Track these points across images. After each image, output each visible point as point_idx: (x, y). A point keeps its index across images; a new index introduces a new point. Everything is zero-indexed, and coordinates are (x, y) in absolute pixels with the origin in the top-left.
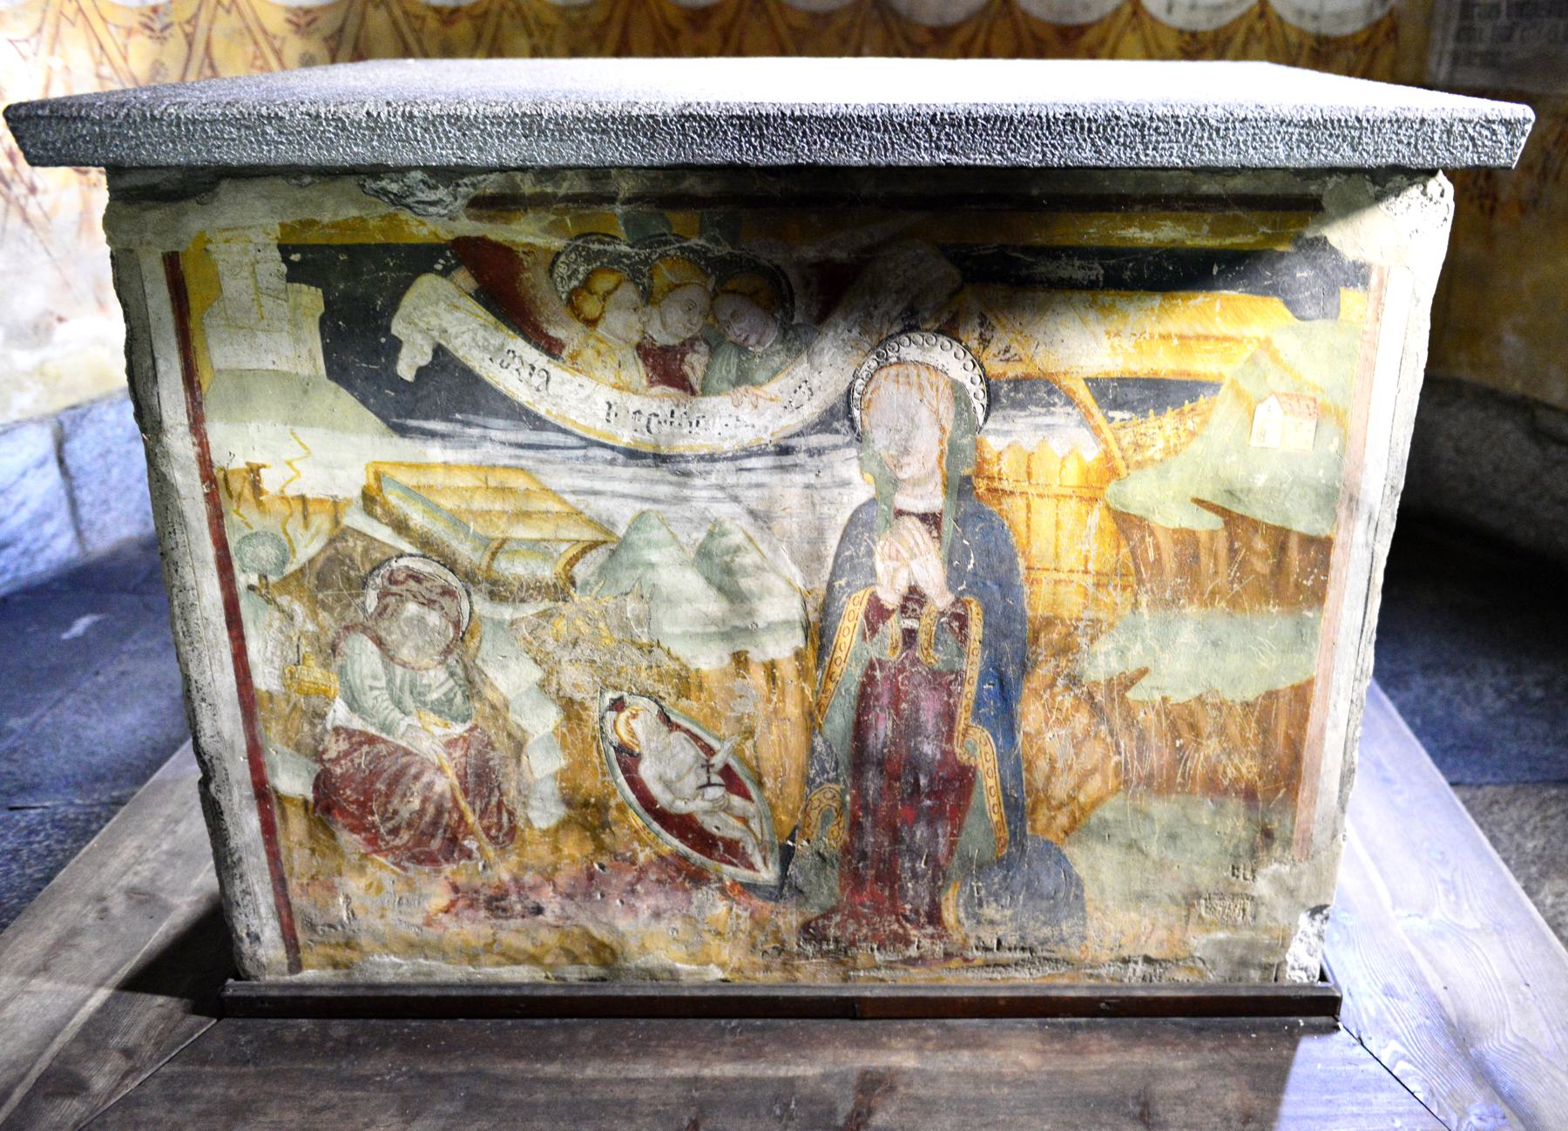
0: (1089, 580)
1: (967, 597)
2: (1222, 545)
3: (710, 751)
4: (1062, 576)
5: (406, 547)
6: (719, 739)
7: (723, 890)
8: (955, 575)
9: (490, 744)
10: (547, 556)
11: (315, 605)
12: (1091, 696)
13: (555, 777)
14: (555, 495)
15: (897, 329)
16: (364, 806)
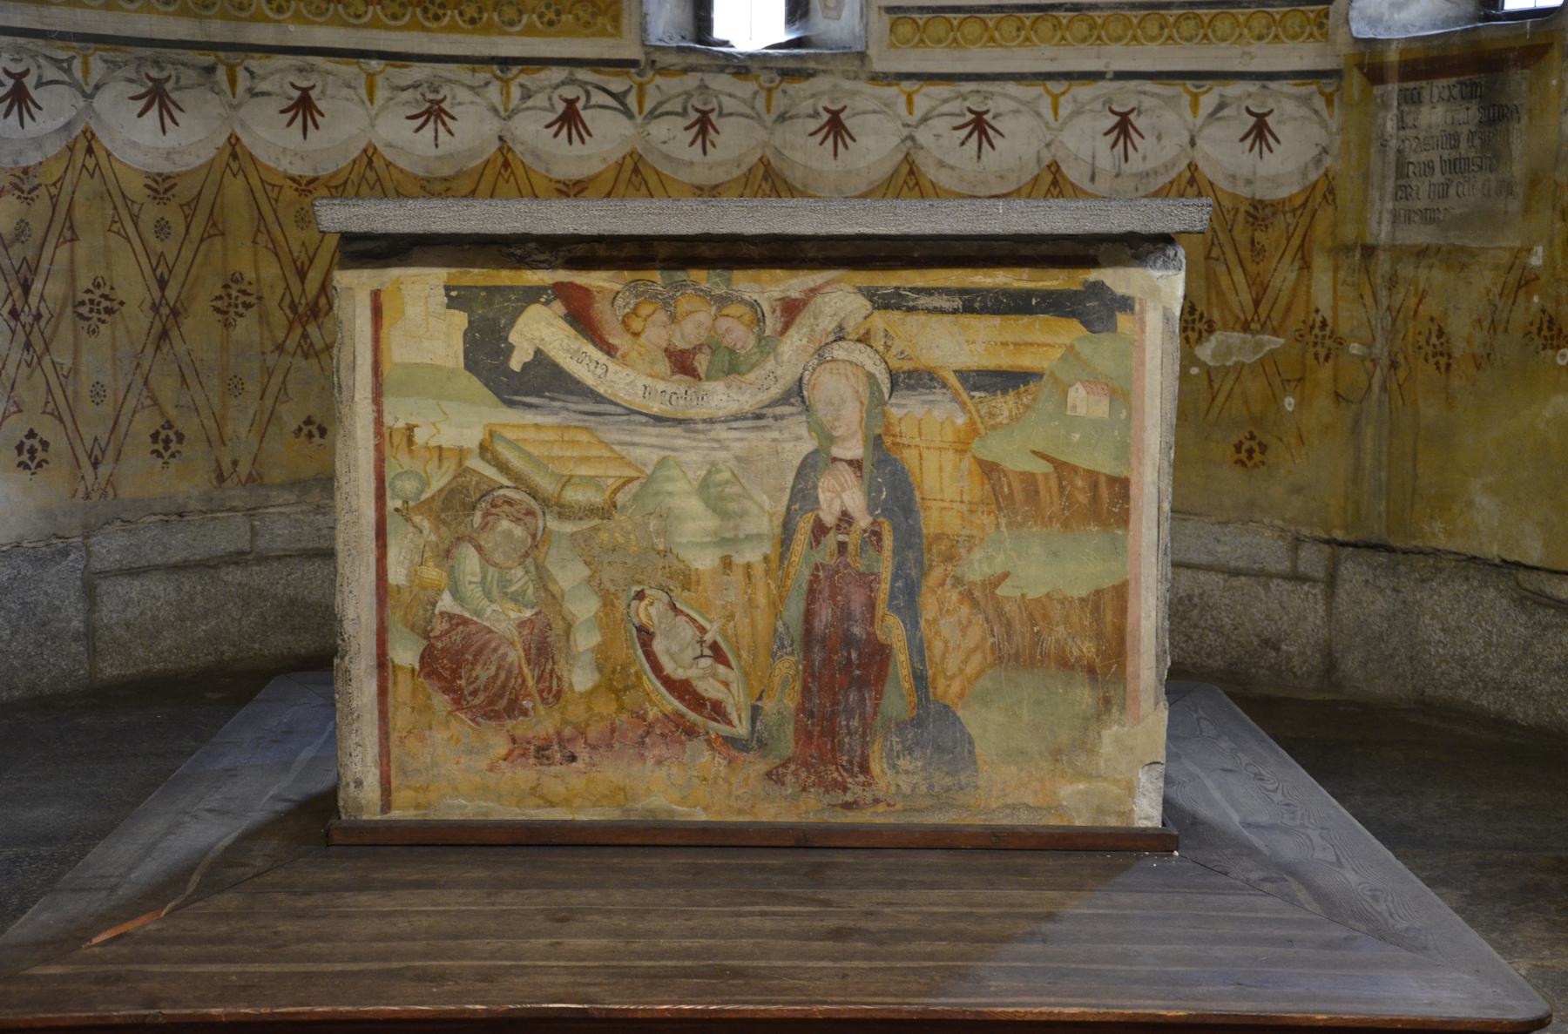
0: (964, 508)
1: (881, 519)
2: (1054, 483)
3: (703, 630)
5: (506, 482)
6: (710, 622)
7: (709, 742)
8: (872, 506)
9: (549, 625)
10: (599, 488)
11: (438, 522)
12: (971, 593)
13: (592, 650)
14: (607, 445)
15: (831, 338)
16: (456, 674)
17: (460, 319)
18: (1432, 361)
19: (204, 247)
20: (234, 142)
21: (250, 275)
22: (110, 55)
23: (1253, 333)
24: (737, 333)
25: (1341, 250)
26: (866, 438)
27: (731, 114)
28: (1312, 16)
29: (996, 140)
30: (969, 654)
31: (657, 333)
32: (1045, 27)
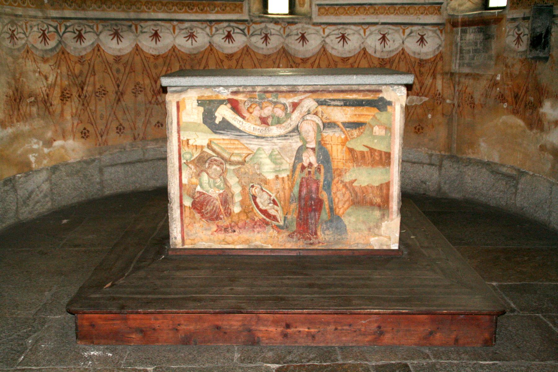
0: (344, 161)
1: (320, 164)
2: (369, 154)
3: (270, 196)
4: (339, 160)
6: (273, 193)
7: (272, 227)
8: (318, 161)
10: (241, 156)
11: (196, 166)
14: (243, 144)
15: (306, 113)
16: (202, 208)
17: (201, 109)
18: (469, 105)
19: (130, 75)
20: (137, 46)
21: (142, 82)
22: (104, 24)
23: (420, 96)
24: (279, 112)
25: (444, 74)
26: (316, 142)
27: (274, 34)
28: (436, 8)
29: (348, 42)
30: (345, 202)
31: (257, 112)
32: (362, 10)
